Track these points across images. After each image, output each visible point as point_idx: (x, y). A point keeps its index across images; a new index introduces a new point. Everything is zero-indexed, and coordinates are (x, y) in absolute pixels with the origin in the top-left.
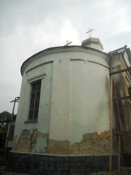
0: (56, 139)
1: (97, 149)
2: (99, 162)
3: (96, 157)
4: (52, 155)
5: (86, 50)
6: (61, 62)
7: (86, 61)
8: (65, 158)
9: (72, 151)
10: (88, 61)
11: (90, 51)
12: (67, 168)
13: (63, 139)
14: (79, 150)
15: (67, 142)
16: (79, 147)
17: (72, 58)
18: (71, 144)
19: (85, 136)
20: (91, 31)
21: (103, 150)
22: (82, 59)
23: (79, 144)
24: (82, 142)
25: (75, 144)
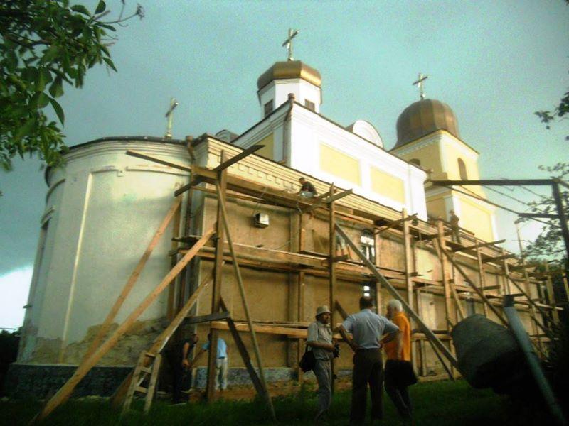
0: (46, 337)
1: (111, 356)
2: (103, 379)
3: (99, 370)
4: (36, 364)
5: (127, 145)
6: (75, 180)
7: (121, 172)
8: (47, 370)
9: (65, 357)
10: (128, 170)
11: (136, 146)
12: (44, 386)
13: (55, 338)
14: (77, 356)
15: (59, 341)
16: (78, 352)
17: (95, 170)
18: (63, 346)
19: (91, 330)
20: (292, 37)
21: (125, 359)
22: (112, 168)
23: (77, 346)
24: (84, 342)
25: (71, 345)
